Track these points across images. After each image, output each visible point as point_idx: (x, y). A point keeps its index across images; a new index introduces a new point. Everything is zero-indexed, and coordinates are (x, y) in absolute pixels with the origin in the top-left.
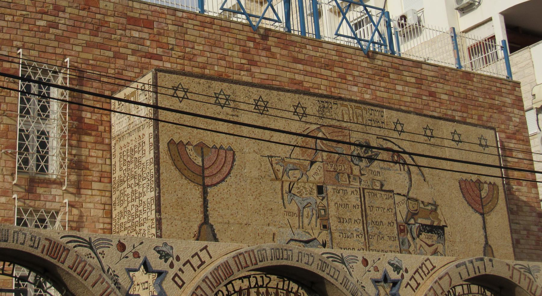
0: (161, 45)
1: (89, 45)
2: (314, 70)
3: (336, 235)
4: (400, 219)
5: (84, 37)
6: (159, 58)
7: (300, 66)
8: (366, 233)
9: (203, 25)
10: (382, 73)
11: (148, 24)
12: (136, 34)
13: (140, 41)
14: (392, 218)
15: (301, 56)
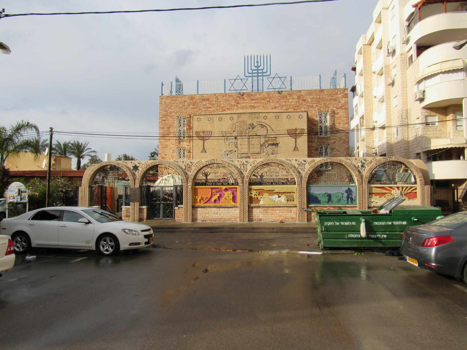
0: (211, 104)
1: (192, 108)
2: (258, 101)
3: (239, 149)
4: (261, 143)
5: (191, 107)
6: (211, 108)
7: (254, 101)
8: (249, 147)
9: (223, 96)
10: (285, 97)
11: (208, 100)
12: (204, 103)
13: (205, 105)
14: (258, 143)
15: (254, 98)
